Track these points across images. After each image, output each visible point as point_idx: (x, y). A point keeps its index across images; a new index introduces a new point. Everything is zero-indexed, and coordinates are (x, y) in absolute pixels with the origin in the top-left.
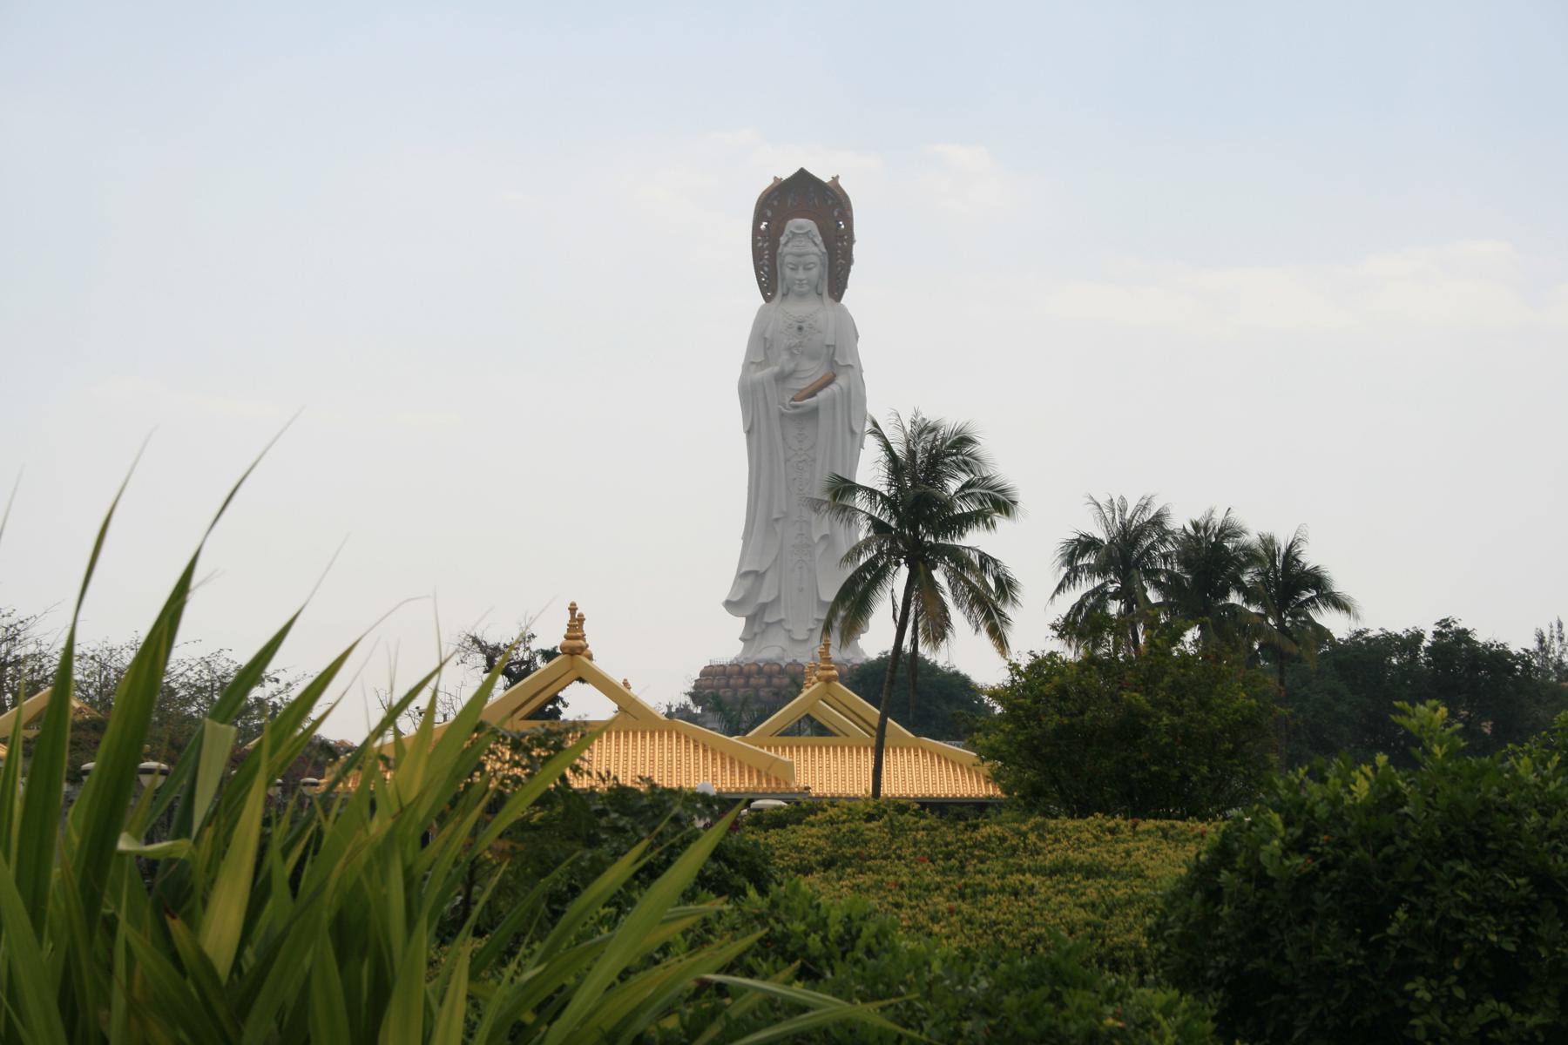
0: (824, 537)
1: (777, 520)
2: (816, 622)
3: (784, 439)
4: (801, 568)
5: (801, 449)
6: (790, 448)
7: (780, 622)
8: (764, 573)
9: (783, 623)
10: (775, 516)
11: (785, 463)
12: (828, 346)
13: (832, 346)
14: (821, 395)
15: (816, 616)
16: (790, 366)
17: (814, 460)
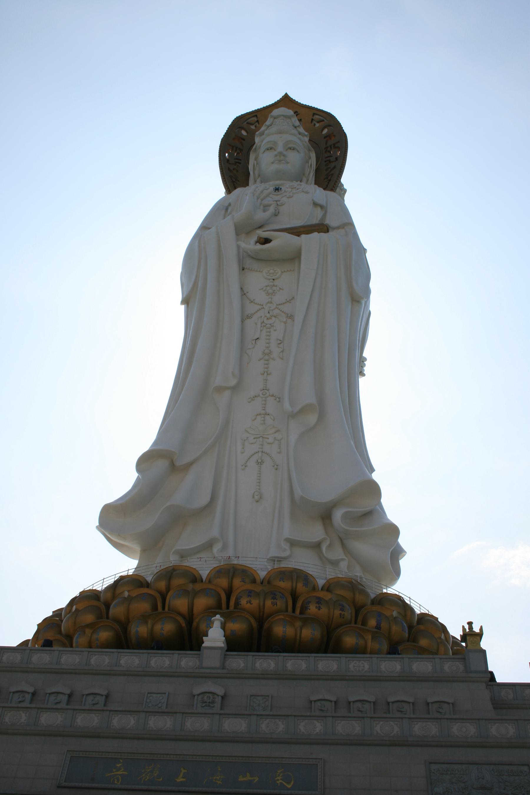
0: (305, 409)
1: (220, 389)
2: (286, 546)
3: (243, 293)
4: (260, 463)
5: (271, 303)
6: (252, 302)
7: (209, 546)
8: (188, 466)
9: (216, 549)
10: (218, 381)
11: (243, 321)
12: (315, 204)
13: (322, 207)
14: (303, 236)
15: (287, 533)
16: (261, 216)
17: (291, 317)
